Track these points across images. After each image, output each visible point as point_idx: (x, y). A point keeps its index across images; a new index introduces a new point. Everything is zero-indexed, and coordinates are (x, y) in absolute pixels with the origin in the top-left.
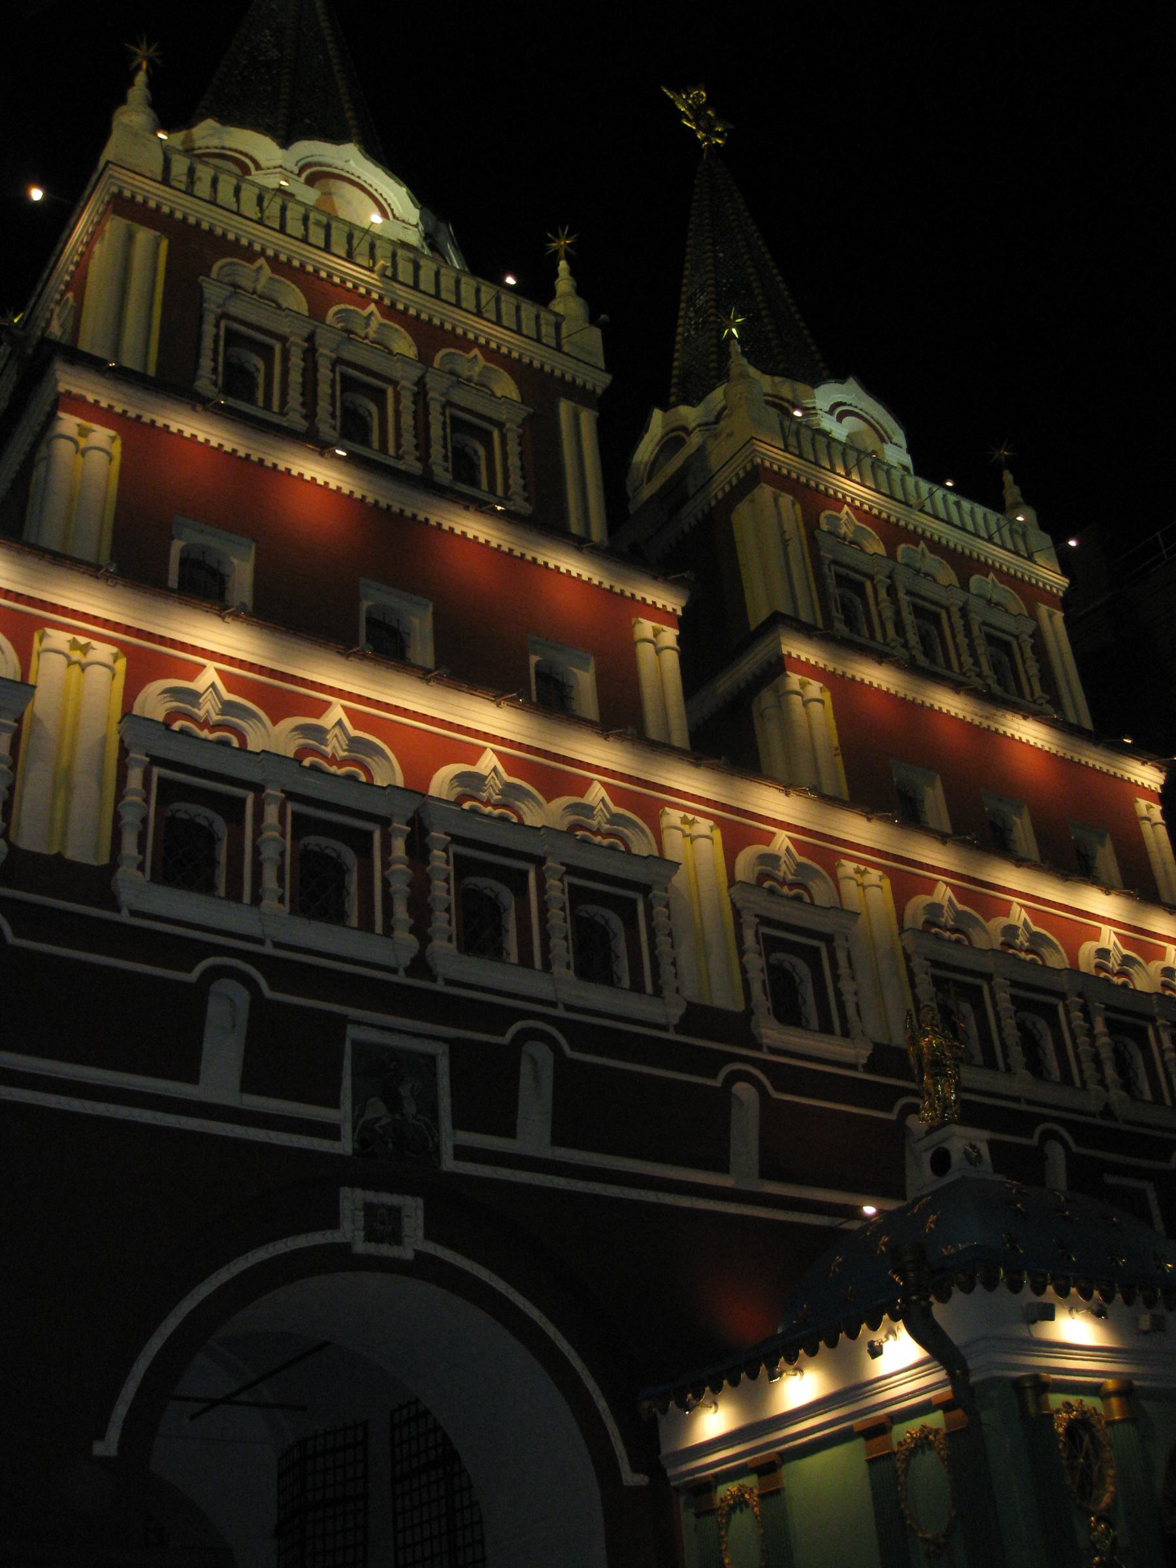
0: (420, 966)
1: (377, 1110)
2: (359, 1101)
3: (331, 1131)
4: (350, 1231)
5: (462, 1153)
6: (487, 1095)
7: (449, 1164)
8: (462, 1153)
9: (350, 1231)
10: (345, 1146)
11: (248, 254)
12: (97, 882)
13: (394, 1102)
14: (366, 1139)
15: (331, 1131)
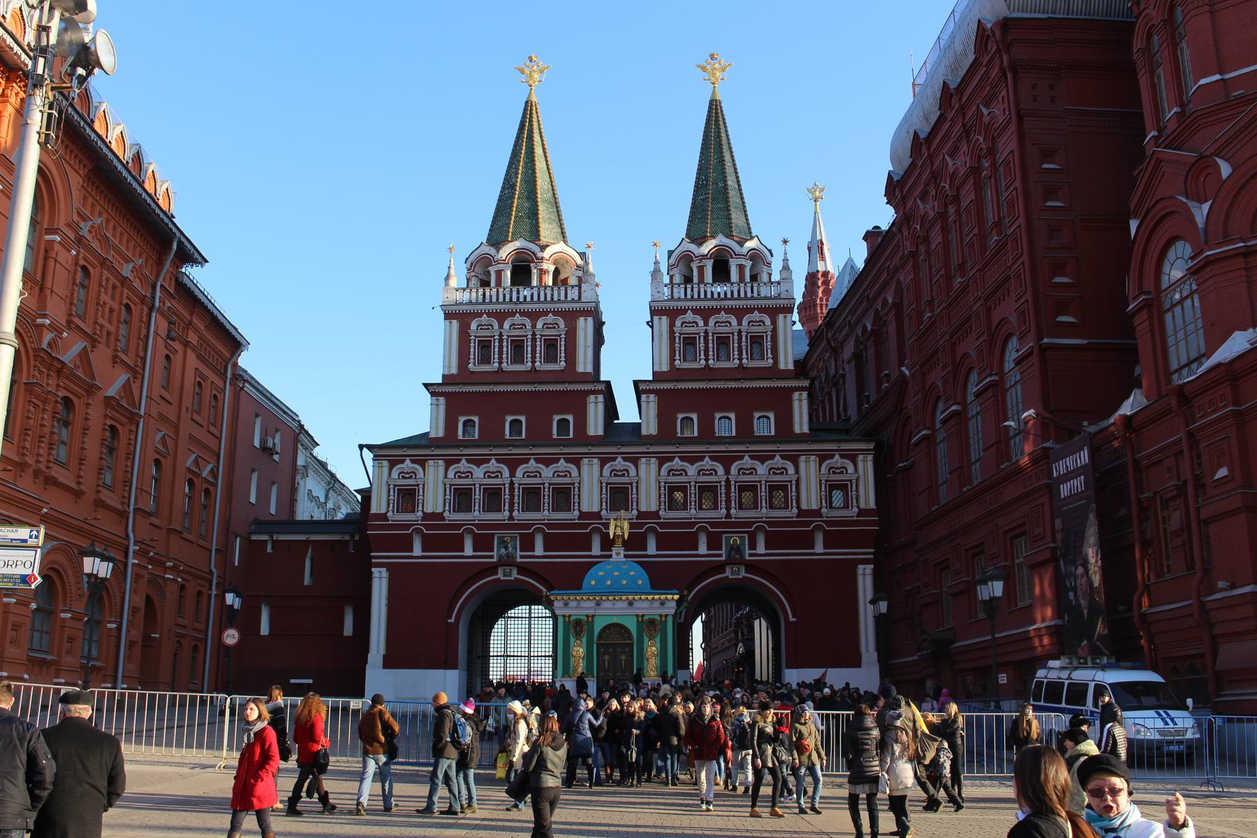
0: (511, 518)
1: (503, 551)
2: (499, 550)
3: (492, 557)
4: (500, 575)
5: (522, 557)
6: (528, 544)
7: (519, 560)
8: (522, 557)
9: (500, 575)
10: (495, 560)
11: (480, 315)
12: (440, 516)
13: (506, 548)
14: (500, 557)
15: (492, 557)
